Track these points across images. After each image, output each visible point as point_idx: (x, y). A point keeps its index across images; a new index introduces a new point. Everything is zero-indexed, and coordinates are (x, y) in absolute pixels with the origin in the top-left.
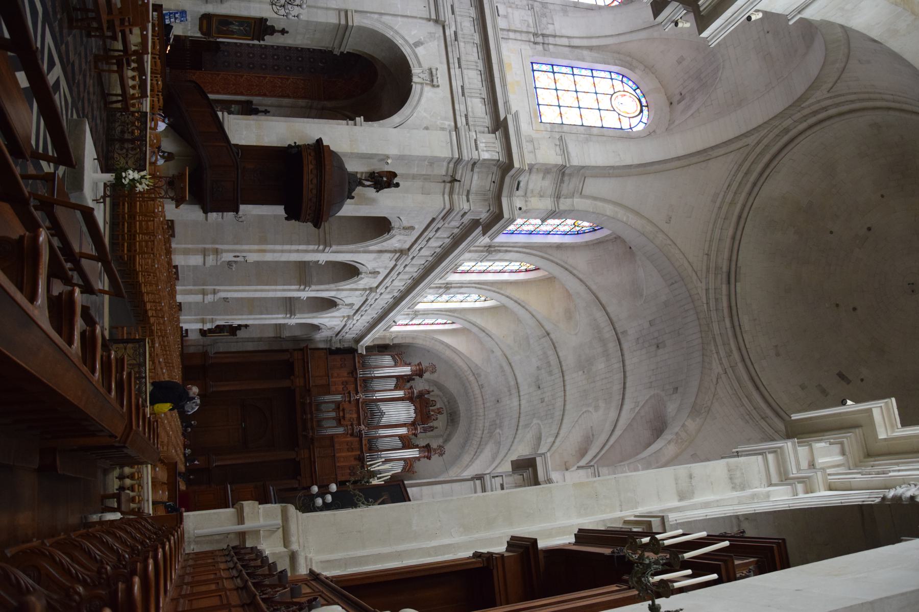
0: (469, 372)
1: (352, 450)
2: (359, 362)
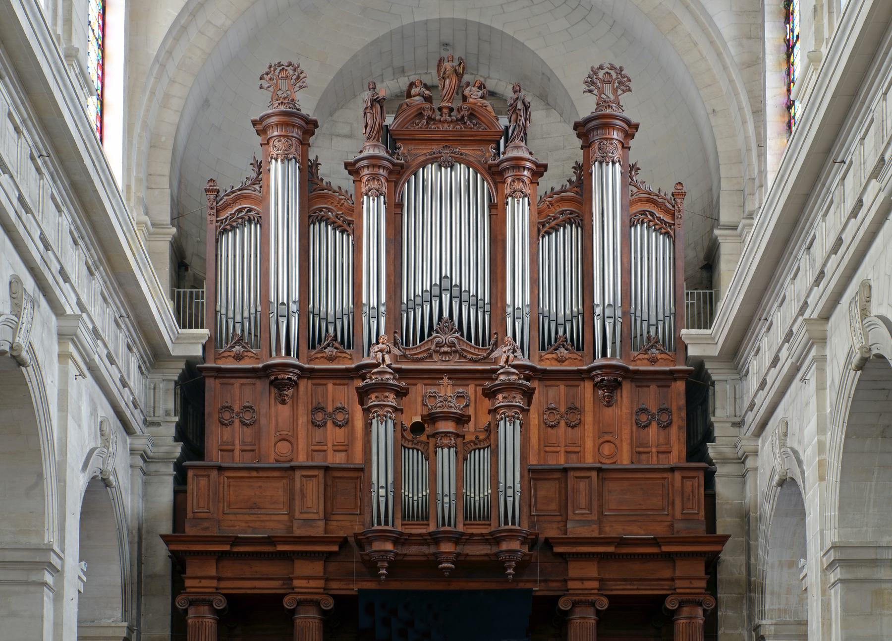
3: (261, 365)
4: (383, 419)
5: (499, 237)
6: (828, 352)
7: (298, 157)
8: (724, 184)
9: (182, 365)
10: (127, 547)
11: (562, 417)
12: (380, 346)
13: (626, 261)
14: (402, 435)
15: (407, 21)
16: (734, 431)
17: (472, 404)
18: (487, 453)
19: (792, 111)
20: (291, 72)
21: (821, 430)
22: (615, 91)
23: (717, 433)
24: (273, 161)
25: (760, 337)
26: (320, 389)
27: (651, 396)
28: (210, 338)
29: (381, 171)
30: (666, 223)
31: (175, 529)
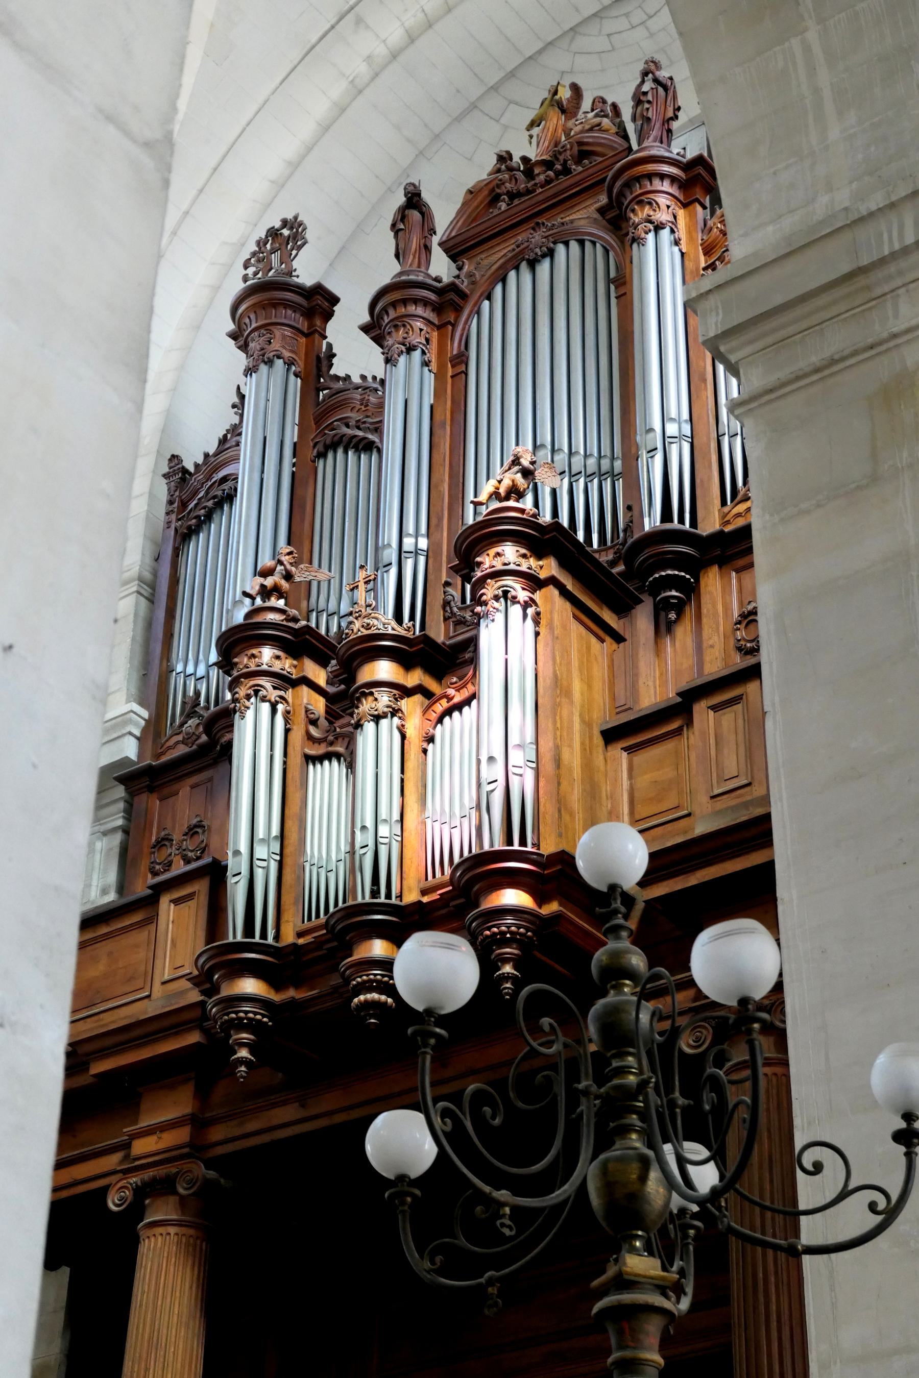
7: (287, 354)
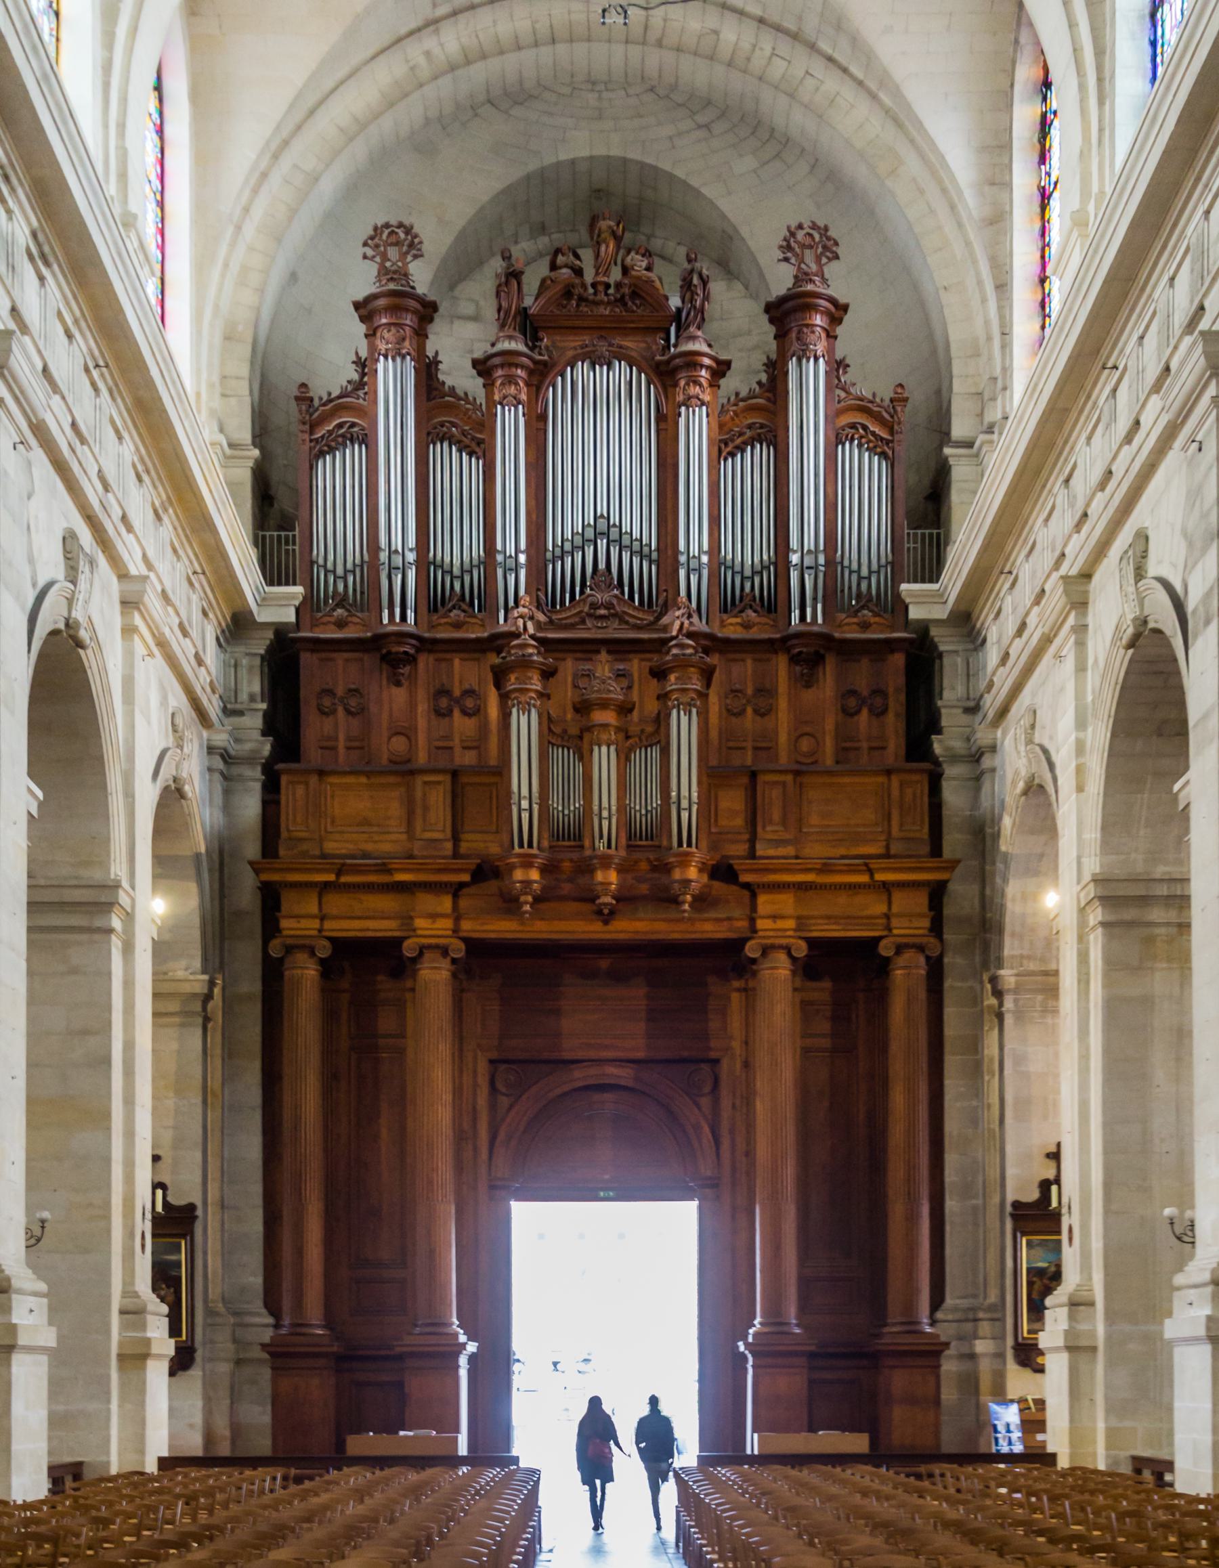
0: (415, 51)
1: (765, 692)
2: (341, 624)
3: (369, 634)
4: (526, 708)
5: (669, 461)
6: (1090, 620)
7: (413, 353)
8: (957, 386)
9: (270, 635)
10: (206, 875)
11: (749, 702)
12: (521, 609)
13: (830, 490)
14: (550, 729)
15: (549, 159)
16: (964, 719)
17: (636, 687)
18: (655, 752)
19: (1047, 285)
20: (402, 236)
21: (1081, 723)
22: (818, 260)
23: (944, 722)
24: (382, 358)
25: (1002, 595)
26: (443, 665)
27: (862, 675)
28: (305, 598)
29: (519, 371)
30: (882, 439)
31: (265, 854)
